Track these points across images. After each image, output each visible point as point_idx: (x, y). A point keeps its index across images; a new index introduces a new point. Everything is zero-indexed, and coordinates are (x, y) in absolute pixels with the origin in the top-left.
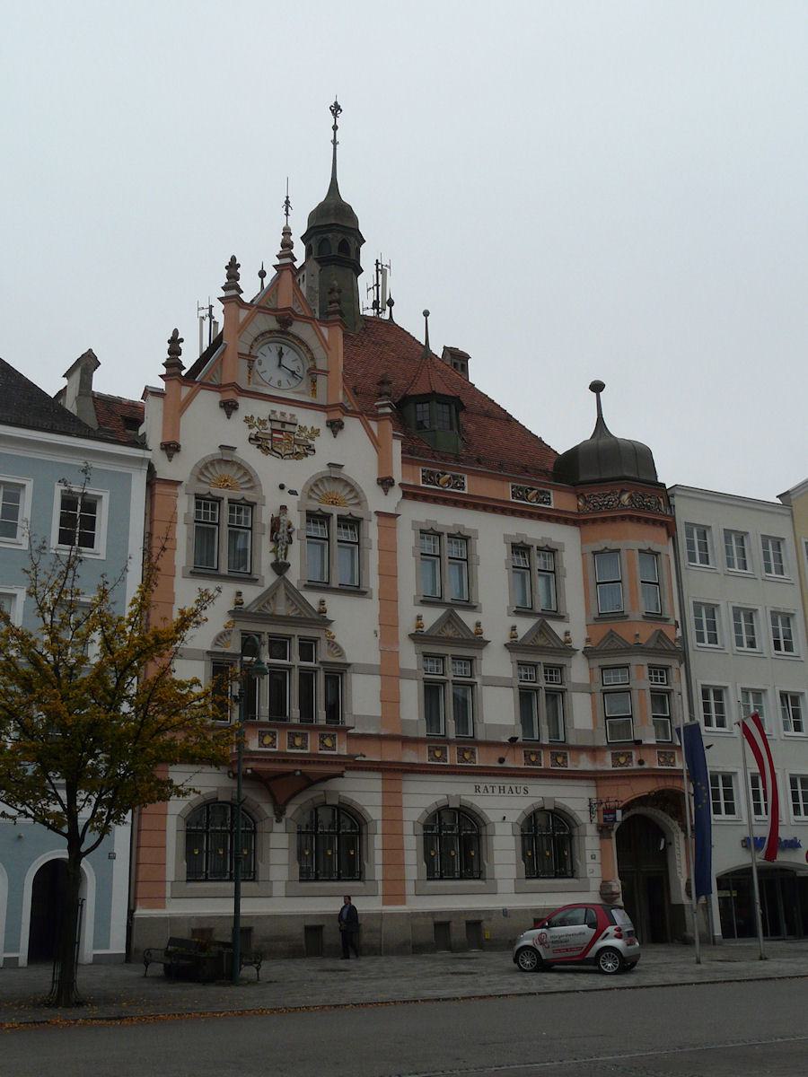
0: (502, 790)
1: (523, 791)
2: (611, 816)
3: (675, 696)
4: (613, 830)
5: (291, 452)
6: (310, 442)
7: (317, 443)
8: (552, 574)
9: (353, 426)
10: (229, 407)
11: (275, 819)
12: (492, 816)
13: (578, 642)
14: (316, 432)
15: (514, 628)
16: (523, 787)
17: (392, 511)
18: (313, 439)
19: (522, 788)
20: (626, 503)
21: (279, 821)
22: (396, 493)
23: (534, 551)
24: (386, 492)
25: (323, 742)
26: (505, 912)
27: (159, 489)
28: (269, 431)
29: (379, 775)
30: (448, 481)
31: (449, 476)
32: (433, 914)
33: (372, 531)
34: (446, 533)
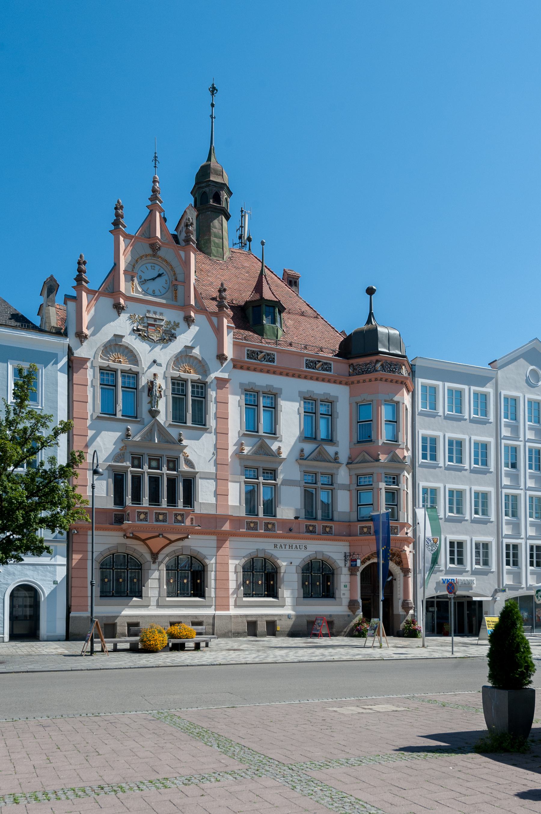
0: (291, 547)
1: (304, 548)
2: (355, 563)
3: (402, 491)
4: (358, 571)
8: (331, 416)
11: (152, 563)
13: (343, 457)
16: (304, 545)
19: (303, 546)
21: (154, 562)
23: (319, 402)
25: (176, 518)
30: (264, 357)
31: (264, 354)
32: (246, 616)
34: (261, 391)
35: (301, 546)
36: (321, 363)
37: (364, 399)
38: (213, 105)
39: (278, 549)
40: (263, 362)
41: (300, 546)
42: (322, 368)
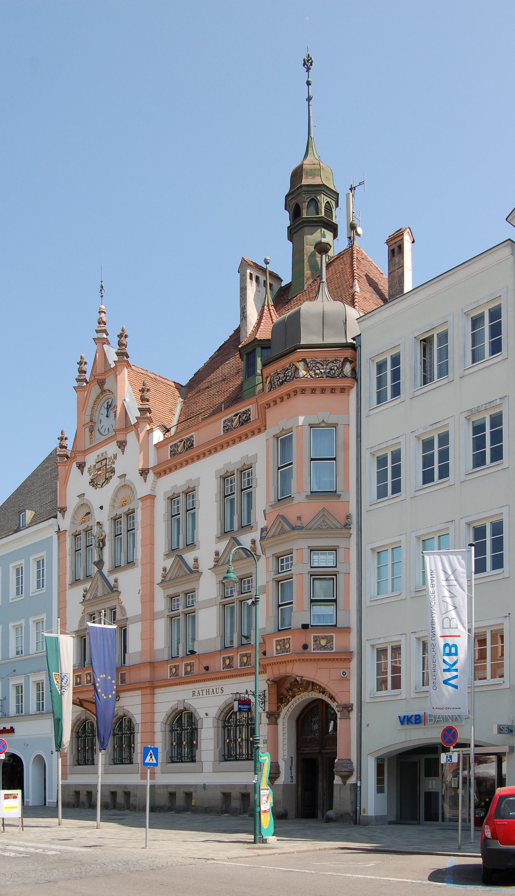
5: (104, 480)
6: (113, 466)
12: (200, 713)
14: (115, 457)
19: (220, 689)
26: (204, 786)
29: (139, 692)
35: (218, 689)
38: (308, 83)
39: (196, 697)
41: (216, 689)
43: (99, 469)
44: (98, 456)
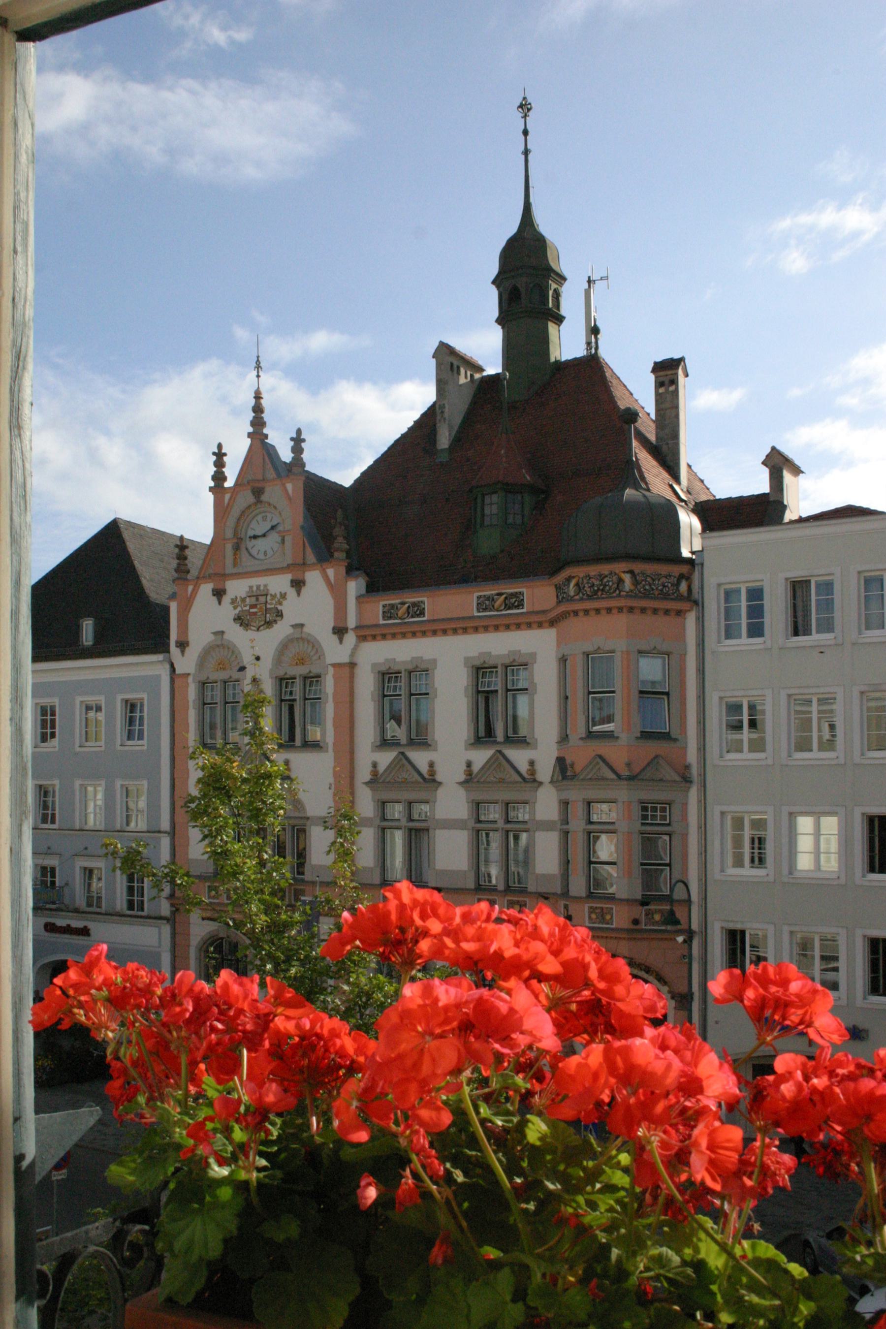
6: (280, 608)
7: (285, 608)
9: (313, 578)
10: (219, 593)
13: (545, 770)
14: (284, 596)
15: (469, 764)
17: (346, 660)
18: (281, 604)
20: (572, 593)
22: (350, 638)
24: (341, 640)
27: (178, 682)
28: (248, 608)
33: (329, 685)
36: (504, 596)
37: (599, 648)
40: (406, 620)
42: (506, 605)
43: (252, 606)
44: (251, 587)
